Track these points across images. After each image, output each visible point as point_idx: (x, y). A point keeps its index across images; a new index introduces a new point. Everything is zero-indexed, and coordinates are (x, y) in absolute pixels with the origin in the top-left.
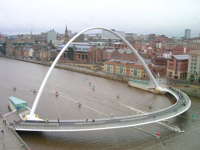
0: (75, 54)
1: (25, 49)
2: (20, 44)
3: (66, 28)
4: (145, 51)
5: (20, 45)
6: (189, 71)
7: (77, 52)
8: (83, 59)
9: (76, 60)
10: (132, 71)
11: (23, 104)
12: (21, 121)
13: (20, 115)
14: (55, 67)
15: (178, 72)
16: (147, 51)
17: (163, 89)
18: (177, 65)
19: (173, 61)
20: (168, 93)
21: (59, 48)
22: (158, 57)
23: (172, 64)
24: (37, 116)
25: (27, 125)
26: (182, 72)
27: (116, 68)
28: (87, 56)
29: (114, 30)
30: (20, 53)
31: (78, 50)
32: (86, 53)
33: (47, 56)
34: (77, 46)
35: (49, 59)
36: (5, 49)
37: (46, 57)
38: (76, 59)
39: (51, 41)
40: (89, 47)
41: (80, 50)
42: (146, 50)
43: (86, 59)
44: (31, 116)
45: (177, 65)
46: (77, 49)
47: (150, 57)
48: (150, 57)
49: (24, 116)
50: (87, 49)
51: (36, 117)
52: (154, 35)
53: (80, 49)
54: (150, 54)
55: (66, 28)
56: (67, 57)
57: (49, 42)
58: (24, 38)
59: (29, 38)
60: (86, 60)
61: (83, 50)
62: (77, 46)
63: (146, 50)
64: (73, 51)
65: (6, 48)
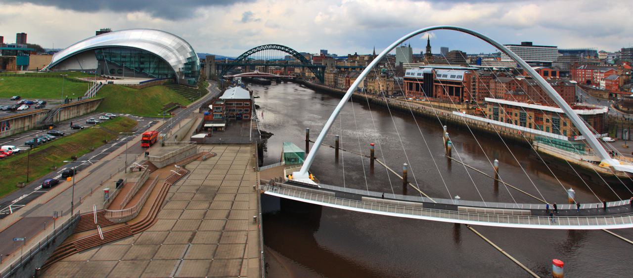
1: (352, 74)
2: (347, 68)
4: (603, 84)
5: (348, 69)
8: (451, 94)
9: (439, 97)
10: (547, 121)
12: (281, 180)
16: (606, 83)
17: (623, 166)
21: (408, 74)
27: (511, 113)
28: (457, 89)
30: (345, 81)
31: (442, 78)
33: (388, 88)
34: (438, 70)
35: (390, 93)
36: (323, 75)
37: (385, 89)
38: (438, 95)
39: (401, 64)
40: (462, 73)
41: (445, 78)
42: (604, 82)
43: (456, 95)
44: (302, 175)
46: (439, 76)
47: (614, 96)
48: (614, 96)
50: (460, 77)
53: (446, 76)
54: (614, 88)
56: (422, 91)
57: (397, 64)
58: (358, 58)
60: (457, 97)
62: (440, 72)
63: (604, 82)
65: (325, 74)
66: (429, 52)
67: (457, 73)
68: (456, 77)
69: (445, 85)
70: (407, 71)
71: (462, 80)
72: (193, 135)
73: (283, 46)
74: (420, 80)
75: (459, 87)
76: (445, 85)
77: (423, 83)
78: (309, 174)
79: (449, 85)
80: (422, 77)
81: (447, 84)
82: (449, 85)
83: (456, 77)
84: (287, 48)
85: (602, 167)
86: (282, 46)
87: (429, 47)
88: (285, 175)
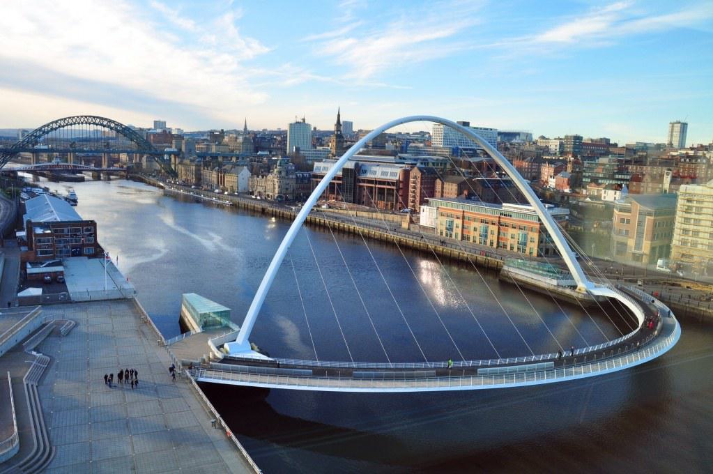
0: (361, 187)
1: (227, 167)
3: (339, 116)
6: (675, 241)
7: (364, 181)
11: (221, 314)
13: (210, 343)
14: (307, 223)
15: (644, 241)
18: (640, 223)
19: (629, 211)
20: (613, 300)
22: (588, 199)
23: (628, 221)
24: (256, 347)
25: (227, 370)
26: (658, 243)
28: (390, 192)
29: (466, 124)
32: (389, 184)
45: (640, 223)
47: (566, 198)
49: (222, 346)
50: (393, 174)
51: (252, 349)
52: (578, 138)
55: (339, 116)
56: (338, 194)
58: (226, 139)
59: (240, 139)
61: (382, 177)
64: (355, 177)
66: (339, 133)
67: (389, 170)
68: (389, 174)
69: (373, 185)
70: (316, 164)
71: (397, 178)
72: (20, 290)
73: (106, 119)
74: (339, 179)
75: (393, 190)
76: (373, 185)
77: (340, 182)
78: (250, 343)
79: (380, 186)
80: (340, 173)
81: (376, 184)
82: (380, 186)
83: (389, 174)
84: (114, 122)
85: (579, 293)
86: (110, 121)
88: (214, 348)
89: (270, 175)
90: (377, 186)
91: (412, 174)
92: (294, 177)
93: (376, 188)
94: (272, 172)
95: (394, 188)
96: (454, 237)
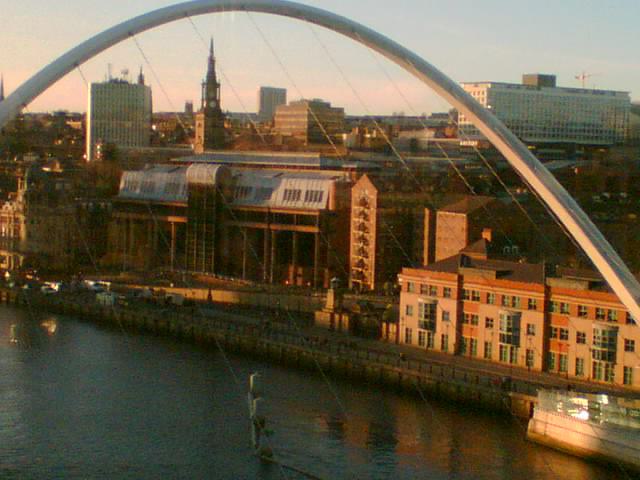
3: (212, 62)
29: (547, 81)
46: (246, 191)
50: (314, 196)
55: (212, 62)
67: (303, 185)
69: (264, 226)
71: (324, 207)
76: (264, 226)
87: (212, 85)
89: (8, 204)
90: (273, 227)
91: (357, 193)
92: (71, 209)
93: (270, 230)
94: (14, 198)
95: (315, 230)
96: (437, 344)
